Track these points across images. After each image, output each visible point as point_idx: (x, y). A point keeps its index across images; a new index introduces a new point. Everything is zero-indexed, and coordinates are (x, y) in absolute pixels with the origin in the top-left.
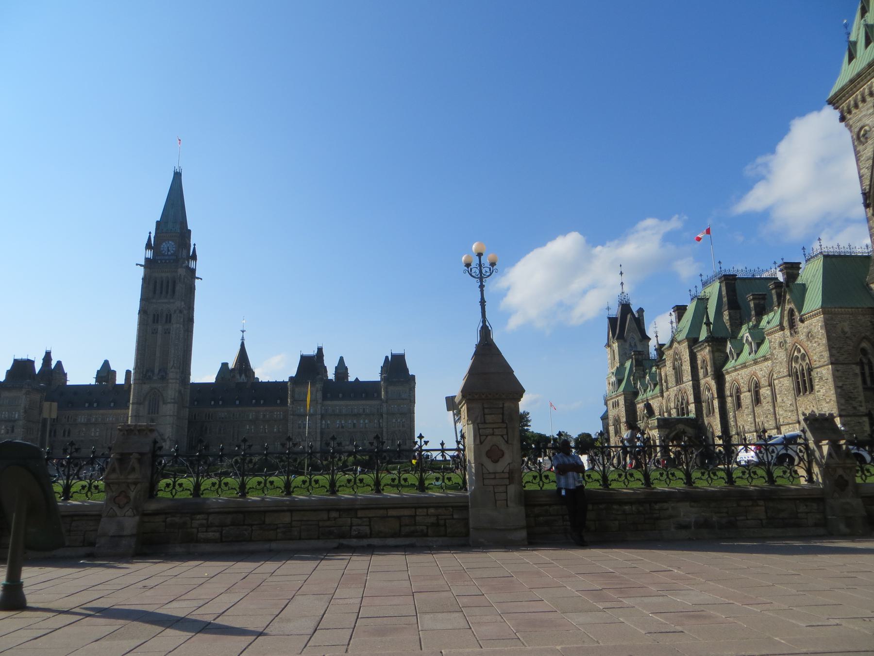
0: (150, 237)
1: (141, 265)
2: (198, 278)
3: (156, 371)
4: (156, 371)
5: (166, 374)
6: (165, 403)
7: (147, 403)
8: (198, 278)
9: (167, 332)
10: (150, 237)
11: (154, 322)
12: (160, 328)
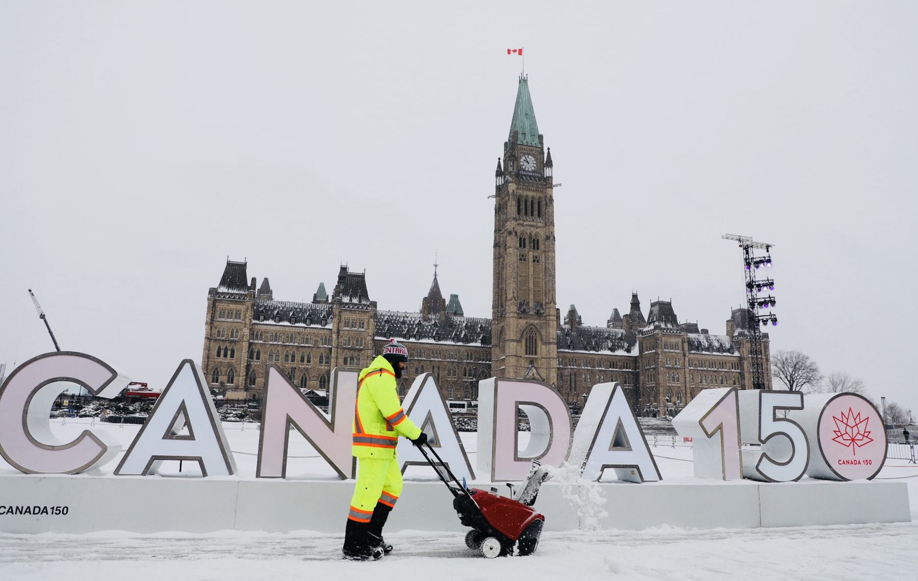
7: (524, 341)
9: (536, 260)
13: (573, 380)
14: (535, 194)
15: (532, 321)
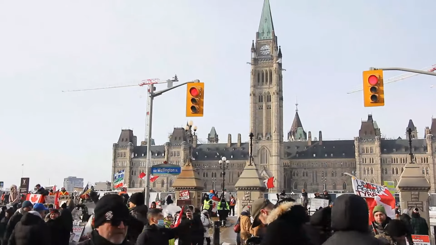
0: (253, 43)
1: (250, 63)
2: (284, 70)
3: (264, 135)
4: (264, 135)
5: (271, 136)
6: (271, 156)
8: (284, 70)
10: (253, 43)
11: (260, 101)
12: (264, 105)
13: (315, 175)
14: (268, 69)
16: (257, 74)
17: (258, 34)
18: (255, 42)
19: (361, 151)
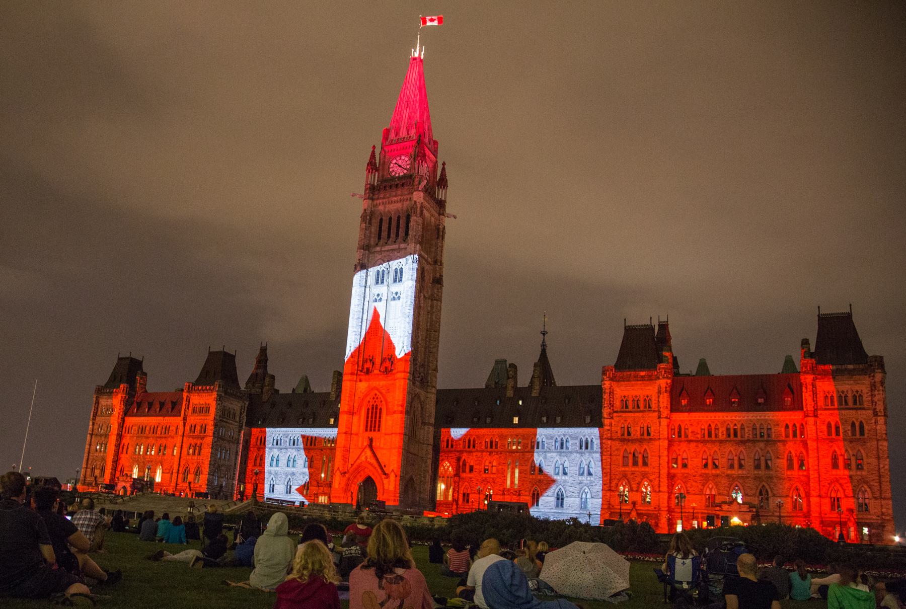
3: (378, 361)
4: (378, 361)
15: (375, 383)
16: (375, 222)
17: (387, 133)
18: (378, 151)
19: (617, 404)
